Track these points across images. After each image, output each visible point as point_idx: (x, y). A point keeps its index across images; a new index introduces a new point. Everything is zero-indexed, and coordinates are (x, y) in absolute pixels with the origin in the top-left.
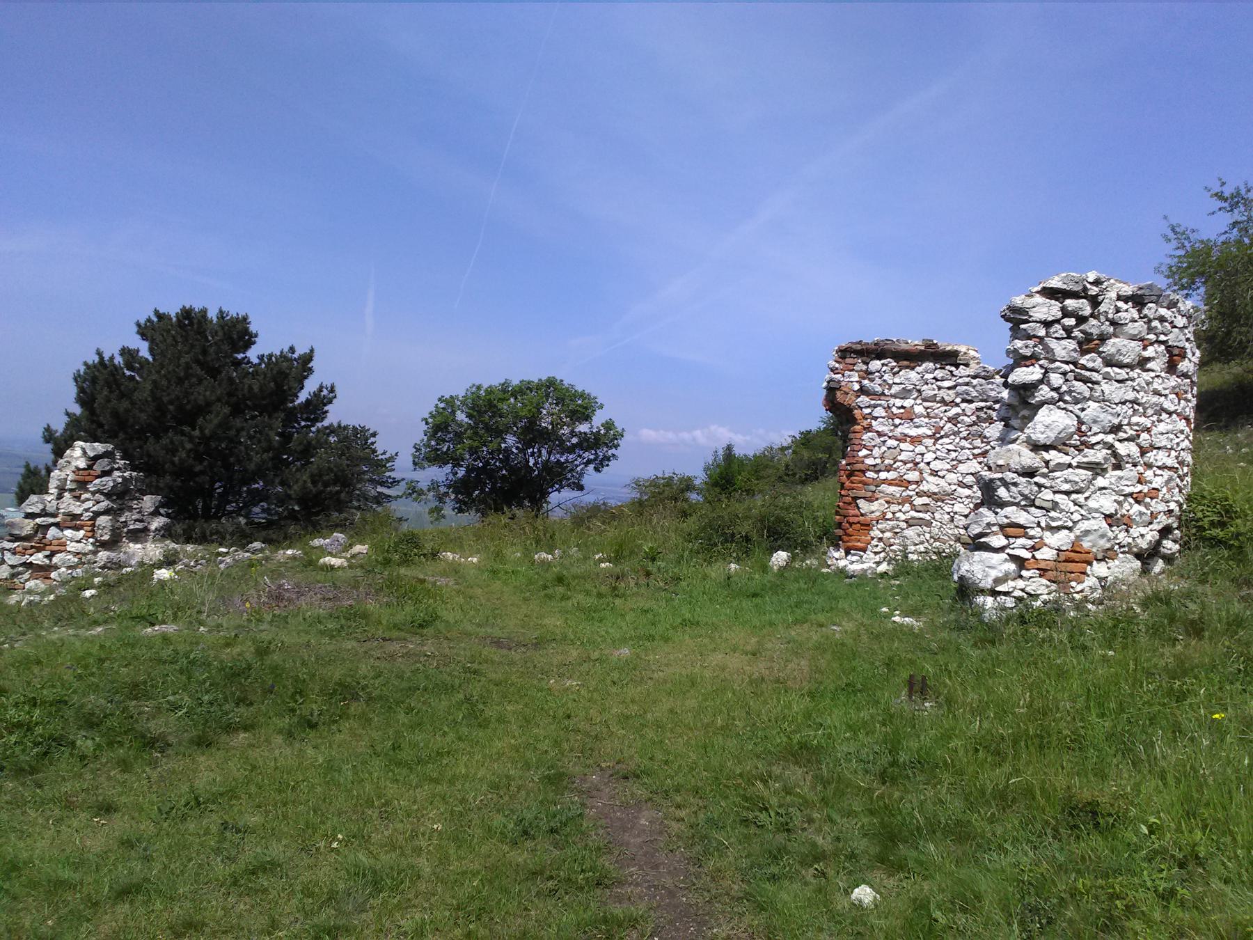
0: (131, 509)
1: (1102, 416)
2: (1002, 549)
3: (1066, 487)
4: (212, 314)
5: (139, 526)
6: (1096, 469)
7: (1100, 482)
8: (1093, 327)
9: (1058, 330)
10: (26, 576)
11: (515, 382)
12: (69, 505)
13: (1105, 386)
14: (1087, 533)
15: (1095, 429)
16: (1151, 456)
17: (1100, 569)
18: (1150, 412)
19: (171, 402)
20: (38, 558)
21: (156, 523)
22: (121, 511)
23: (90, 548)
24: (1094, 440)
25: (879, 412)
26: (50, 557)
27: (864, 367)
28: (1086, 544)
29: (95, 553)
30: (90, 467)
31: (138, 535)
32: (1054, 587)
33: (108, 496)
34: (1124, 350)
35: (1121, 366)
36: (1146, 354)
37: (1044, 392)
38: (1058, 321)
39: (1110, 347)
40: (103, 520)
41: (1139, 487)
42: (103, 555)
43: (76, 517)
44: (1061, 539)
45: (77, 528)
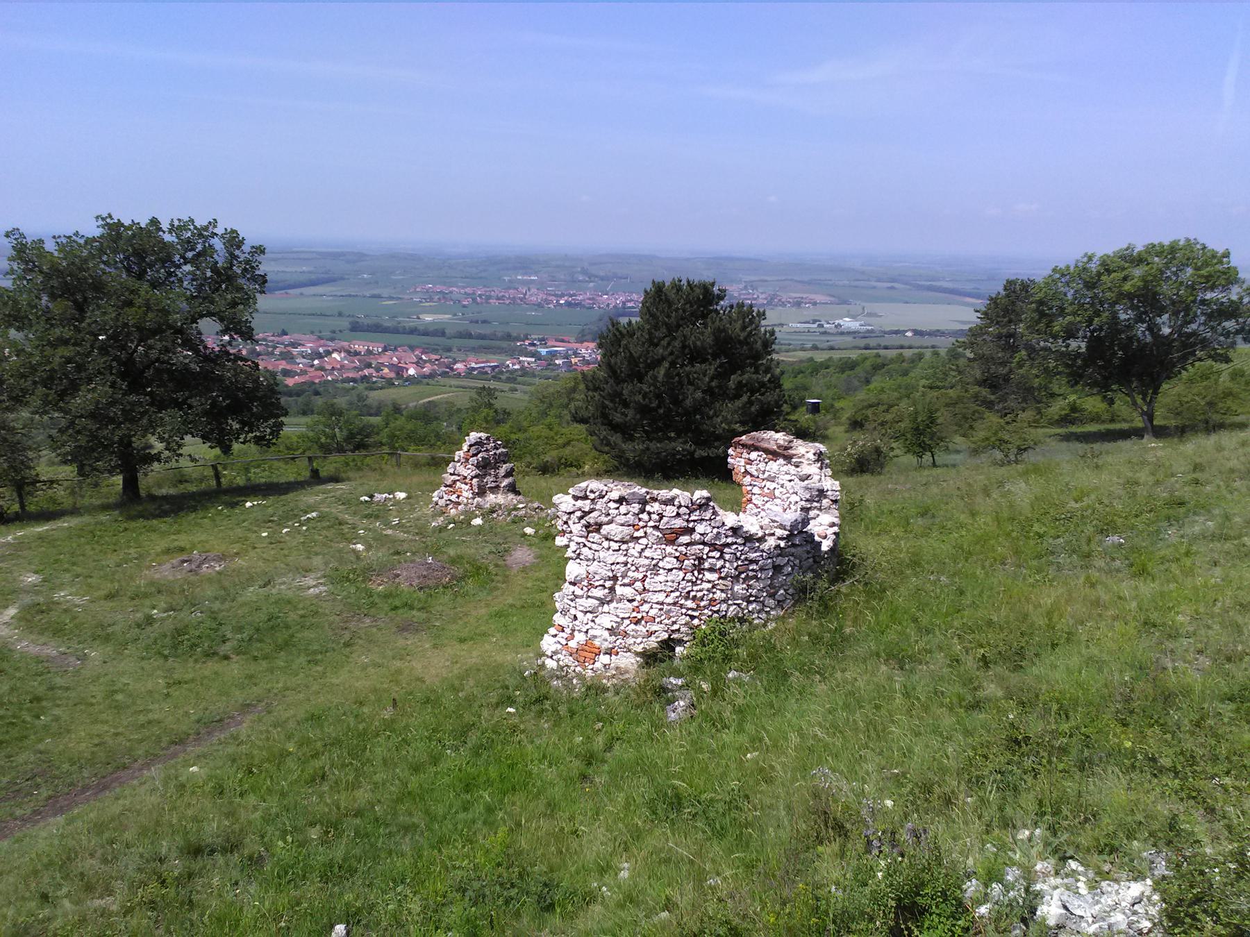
0: (490, 475)
1: (600, 571)
2: (555, 636)
3: (581, 608)
4: (684, 282)
5: (493, 485)
6: (603, 602)
7: (606, 608)
8: (591, 518)
9: (574, 517)
10: (451, 506)
11: (1139, 247)
12: (465, 472)
13: (602, 554)
14: (595, 637)
15: (597, 577)
16: (648, 596)
17: (604, 659)
18: (641, 569)
19: (639, 358)
20: (453, 498)
21: (505, 482)
22: (485, 475)
23: (471, 496)
24: (597, 584)
25: (756, 490)
26: (458, 497)
27: (747, 456)
28: (597, 642)
29: (474, 498)
30: (469, 451)
31: (495, 489)
32: (577, 663)
33: (478, 467)
34: (613, 533)
35: (616, 542)
36: (637, 534)
37: (569, 554)
38: (573, 512)
39: (605, 529)
40: (475, 480)
41: (634, 614)
42: (478, 499)
43: (465, 478)
44: (580, 638)
45: (466, 484)
